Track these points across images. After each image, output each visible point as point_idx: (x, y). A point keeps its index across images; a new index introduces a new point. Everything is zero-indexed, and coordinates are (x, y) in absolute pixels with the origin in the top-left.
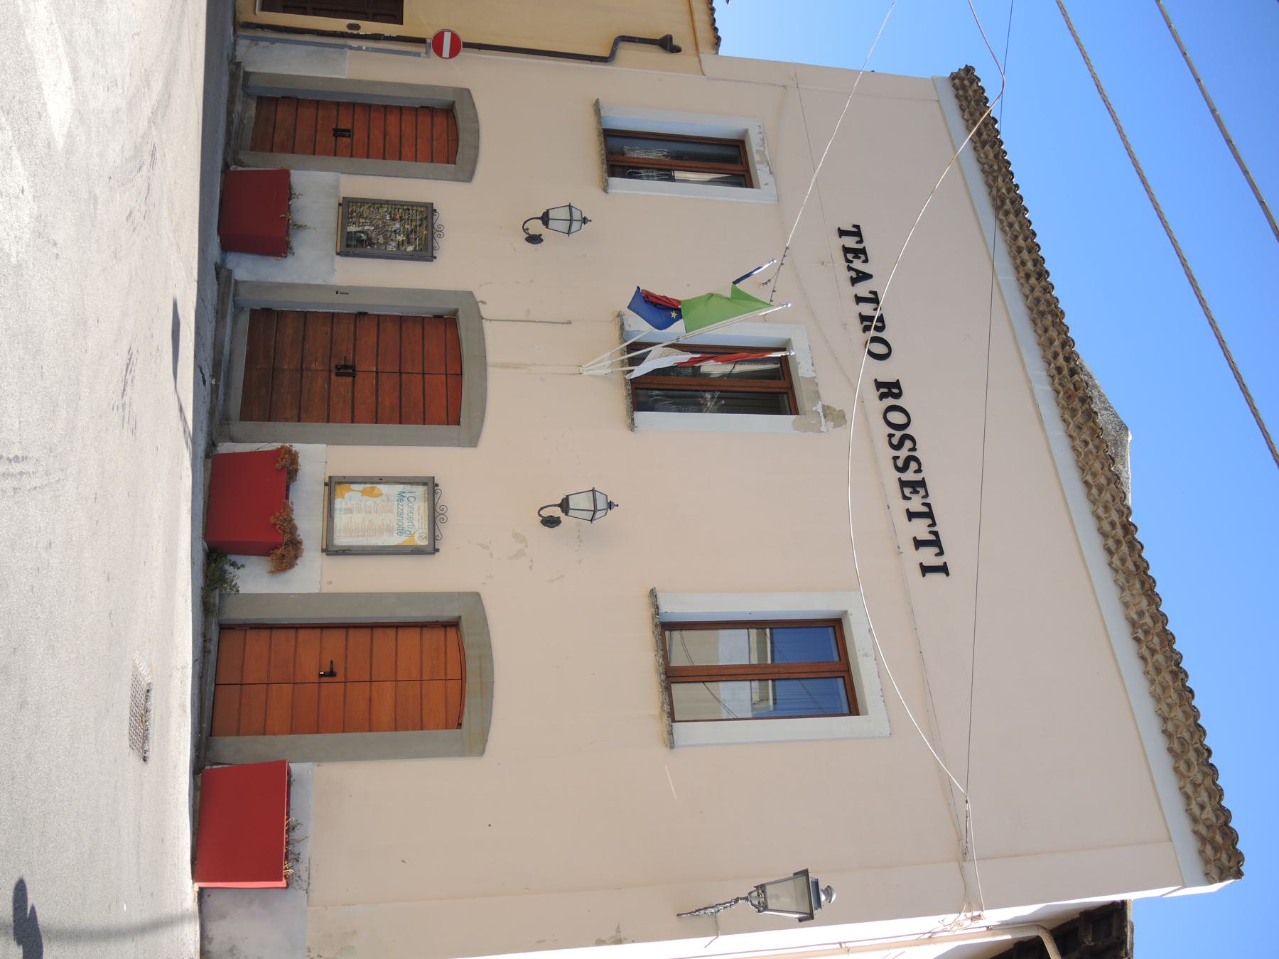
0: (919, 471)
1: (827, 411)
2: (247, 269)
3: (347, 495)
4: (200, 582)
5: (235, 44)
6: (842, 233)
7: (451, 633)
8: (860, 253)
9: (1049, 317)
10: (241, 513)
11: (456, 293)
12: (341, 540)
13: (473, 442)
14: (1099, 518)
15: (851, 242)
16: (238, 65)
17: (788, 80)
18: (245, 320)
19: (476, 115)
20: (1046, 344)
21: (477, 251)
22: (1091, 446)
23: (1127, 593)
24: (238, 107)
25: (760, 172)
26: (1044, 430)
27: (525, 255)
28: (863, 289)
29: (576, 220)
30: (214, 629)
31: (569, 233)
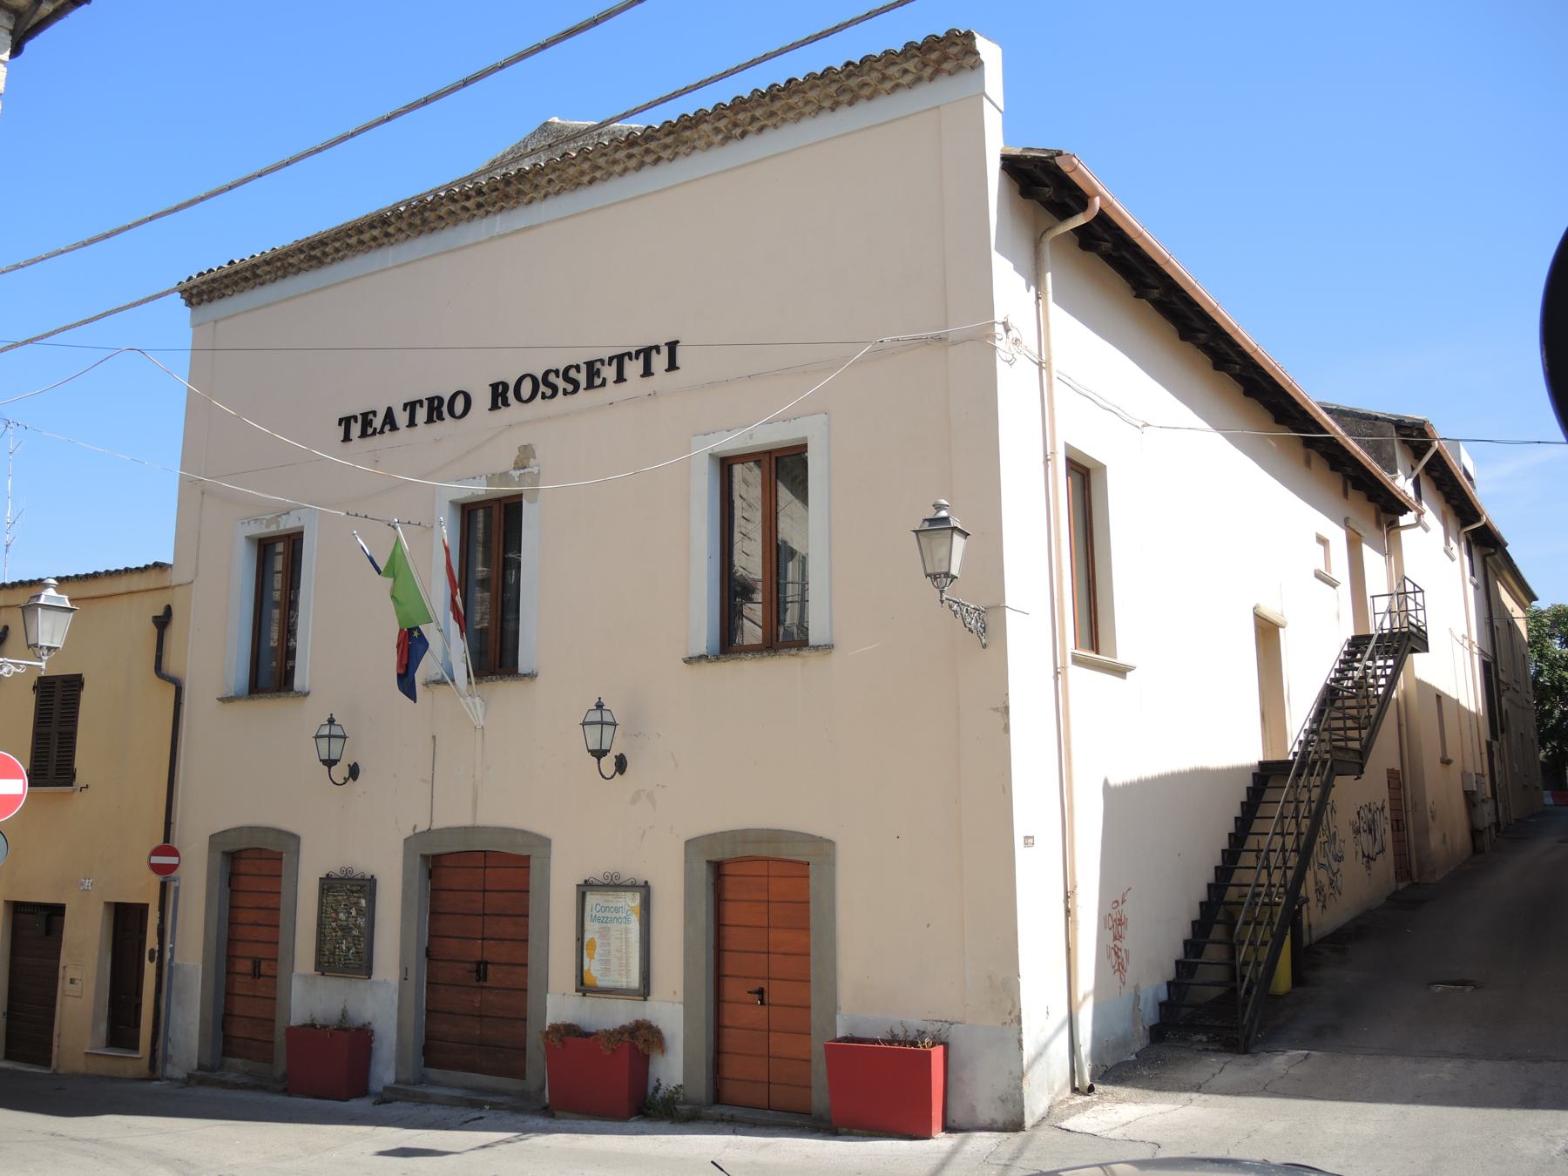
0: (578, 368)
1: (520, 465)
2: (384, 1072)
3: (594, 973)
4: (664, 1125)
5: (170, 1079)
6: (347, 438)
7: (728, 869)
8: (366, 419)
9: (427, 214)
10: (608, 1083)
11: (405, 855)
12: (634, 981)
13: (546, 842)
14: (626, 170)
15: (356, 429)
16: (190, 1076)
17: (196, 497)
18: (434, 1073)
19: (234, 830)
20: (453, 219)
21: (363, 835)
22: (552, 177)
23: (697, 143)
24: (231, 1076)
25: (288, 524)
26: (540, 225)
27: (372, 784)
28: (402, 418)
29: (332, 731)
30: (717, 1110)
31: (345, 737)
